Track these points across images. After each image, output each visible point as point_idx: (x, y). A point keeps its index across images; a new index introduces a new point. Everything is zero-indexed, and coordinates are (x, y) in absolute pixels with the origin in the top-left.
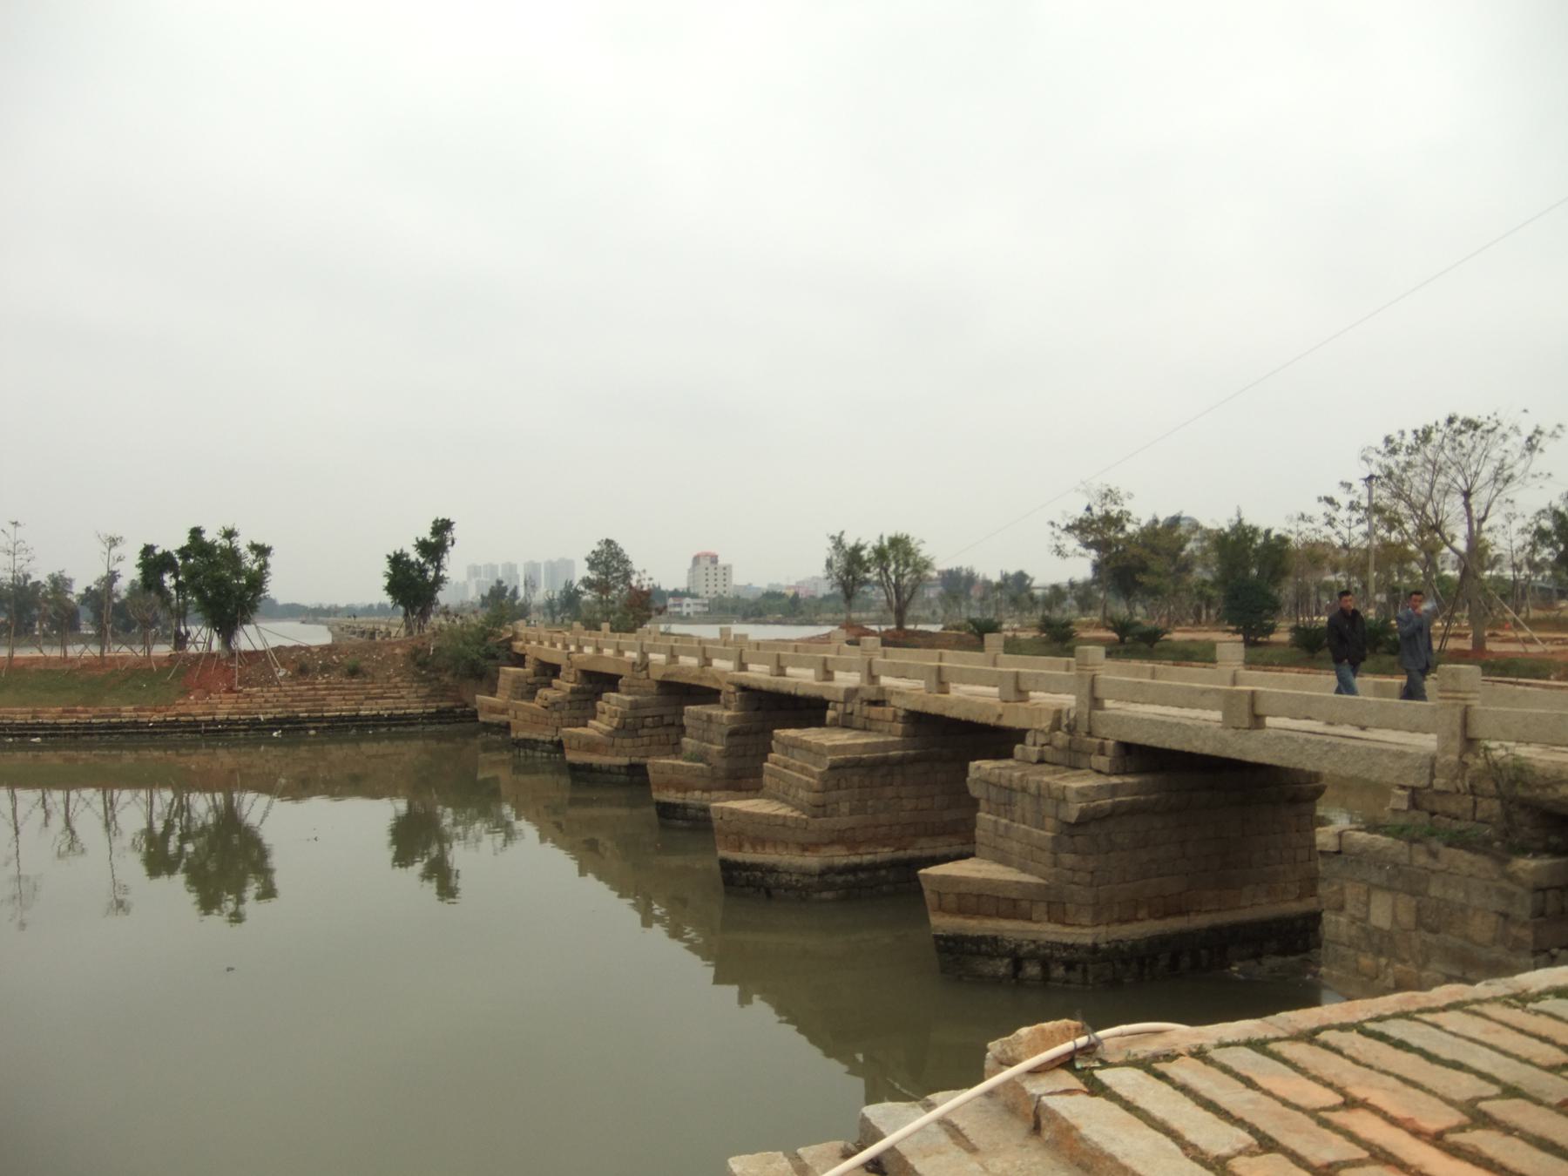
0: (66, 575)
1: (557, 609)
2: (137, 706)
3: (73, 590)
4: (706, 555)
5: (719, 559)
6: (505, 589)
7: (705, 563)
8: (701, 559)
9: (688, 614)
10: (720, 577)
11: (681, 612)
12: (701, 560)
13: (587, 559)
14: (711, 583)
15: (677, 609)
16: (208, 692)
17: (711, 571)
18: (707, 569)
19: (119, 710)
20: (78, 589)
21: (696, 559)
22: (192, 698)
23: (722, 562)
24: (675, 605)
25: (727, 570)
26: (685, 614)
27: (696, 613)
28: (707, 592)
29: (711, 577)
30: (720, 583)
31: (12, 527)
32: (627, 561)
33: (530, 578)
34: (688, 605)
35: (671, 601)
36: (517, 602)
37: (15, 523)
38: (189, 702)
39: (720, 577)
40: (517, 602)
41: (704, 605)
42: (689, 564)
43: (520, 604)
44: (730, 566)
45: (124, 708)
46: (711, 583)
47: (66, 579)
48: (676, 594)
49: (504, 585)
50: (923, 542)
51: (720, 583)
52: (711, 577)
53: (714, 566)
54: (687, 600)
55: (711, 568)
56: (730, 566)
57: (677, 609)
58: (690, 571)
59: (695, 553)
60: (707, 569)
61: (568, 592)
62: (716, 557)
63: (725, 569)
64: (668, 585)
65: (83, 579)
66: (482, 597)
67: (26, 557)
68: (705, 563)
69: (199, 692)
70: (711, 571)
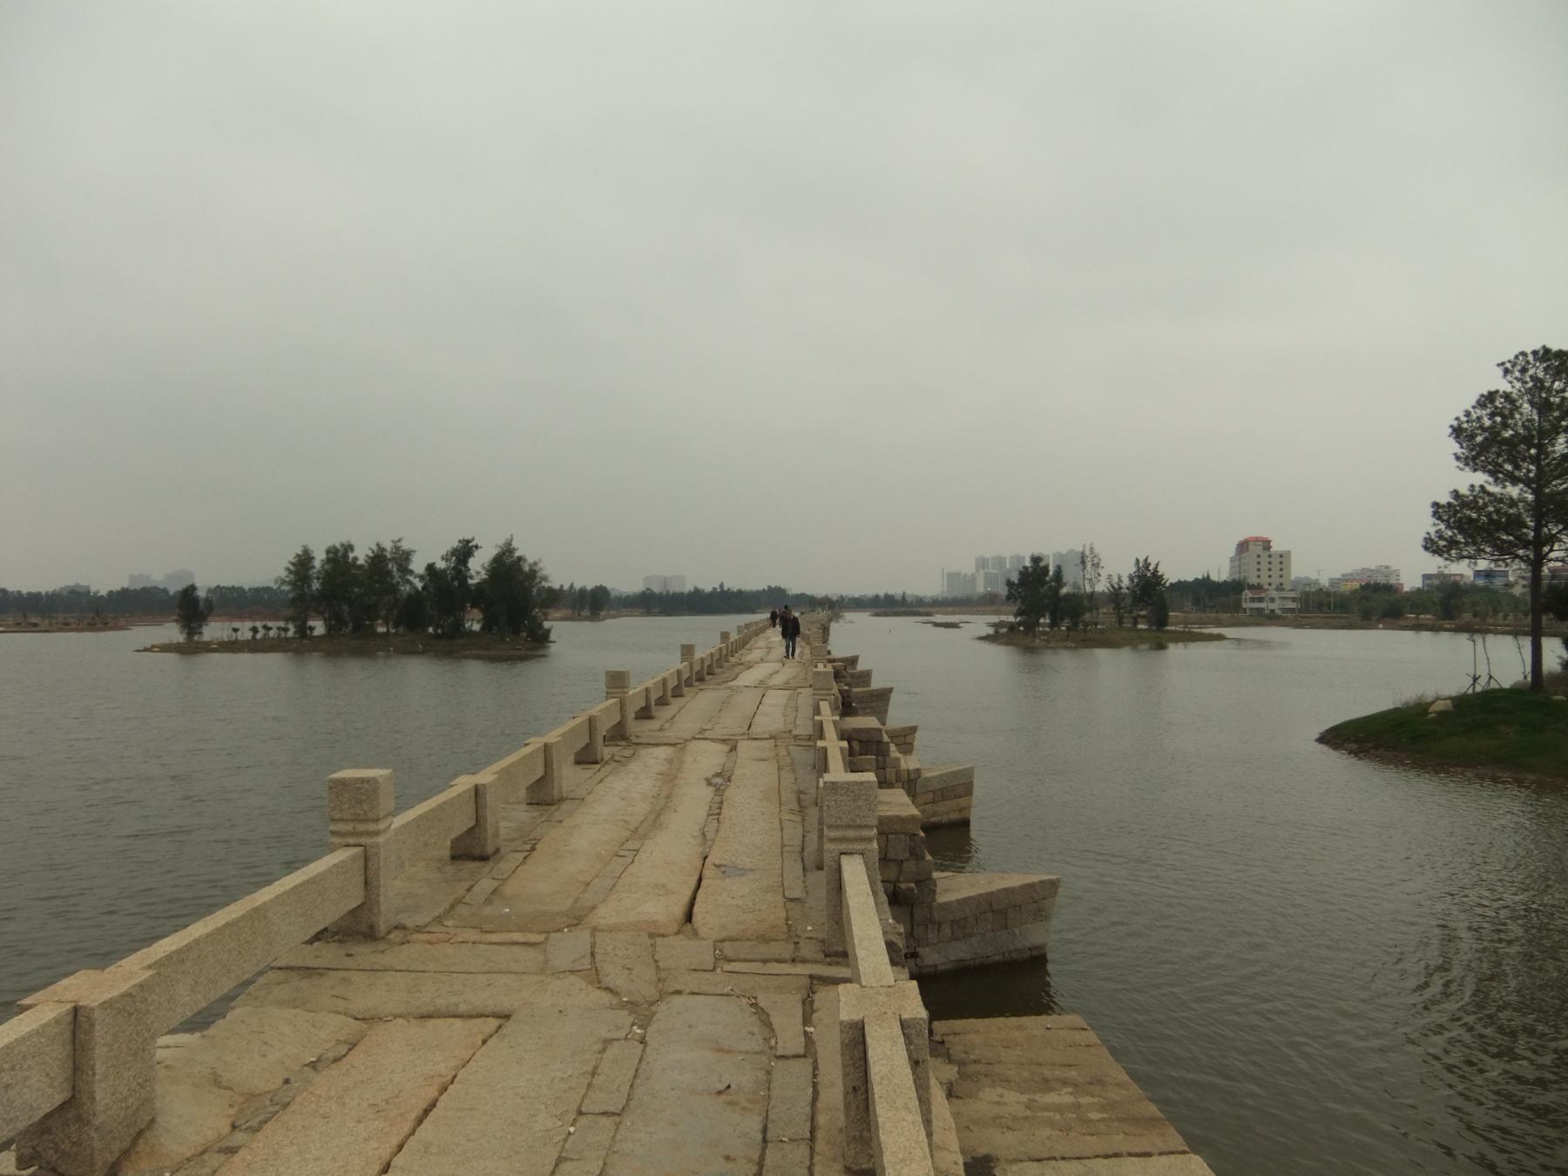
0: (405, 546)
1: (1129, 601)
3: (412, 567)
4: (1256, 540)
5: (1272, 544)
6: (1046, 569)
8: (1250, 543)
10: (1275, 566)
11: (1260, 610)
12: (1251, 547)
13: (1457, 432)
14: (1264, 573)
17: (1264, 559)
18: (1259, 556)
20: (418, 566)
21: (1243, 546)
23: (1276, 547)
24: (1253, 600)
25: (1284, 557)
29: (1264, 566)
30: (1275, 573)
33: (1092, 549)
39: (1275, 566)
40: (1064, 591)
41: (1294, 600)
42: (1232, 552)
46: (1264, 573)
47: (403, 551)
49: (1042, 564)
51: (1275, 573)
52: (1264, 566)
53: (1267, 553)
55: (1264, 555)
58: (1232, 560)
59: (1242, 539)
63: (1281, 556)
65: (429, 553)
66: (1009, 584)
68: (1255, 549)
70: (1264, 559)
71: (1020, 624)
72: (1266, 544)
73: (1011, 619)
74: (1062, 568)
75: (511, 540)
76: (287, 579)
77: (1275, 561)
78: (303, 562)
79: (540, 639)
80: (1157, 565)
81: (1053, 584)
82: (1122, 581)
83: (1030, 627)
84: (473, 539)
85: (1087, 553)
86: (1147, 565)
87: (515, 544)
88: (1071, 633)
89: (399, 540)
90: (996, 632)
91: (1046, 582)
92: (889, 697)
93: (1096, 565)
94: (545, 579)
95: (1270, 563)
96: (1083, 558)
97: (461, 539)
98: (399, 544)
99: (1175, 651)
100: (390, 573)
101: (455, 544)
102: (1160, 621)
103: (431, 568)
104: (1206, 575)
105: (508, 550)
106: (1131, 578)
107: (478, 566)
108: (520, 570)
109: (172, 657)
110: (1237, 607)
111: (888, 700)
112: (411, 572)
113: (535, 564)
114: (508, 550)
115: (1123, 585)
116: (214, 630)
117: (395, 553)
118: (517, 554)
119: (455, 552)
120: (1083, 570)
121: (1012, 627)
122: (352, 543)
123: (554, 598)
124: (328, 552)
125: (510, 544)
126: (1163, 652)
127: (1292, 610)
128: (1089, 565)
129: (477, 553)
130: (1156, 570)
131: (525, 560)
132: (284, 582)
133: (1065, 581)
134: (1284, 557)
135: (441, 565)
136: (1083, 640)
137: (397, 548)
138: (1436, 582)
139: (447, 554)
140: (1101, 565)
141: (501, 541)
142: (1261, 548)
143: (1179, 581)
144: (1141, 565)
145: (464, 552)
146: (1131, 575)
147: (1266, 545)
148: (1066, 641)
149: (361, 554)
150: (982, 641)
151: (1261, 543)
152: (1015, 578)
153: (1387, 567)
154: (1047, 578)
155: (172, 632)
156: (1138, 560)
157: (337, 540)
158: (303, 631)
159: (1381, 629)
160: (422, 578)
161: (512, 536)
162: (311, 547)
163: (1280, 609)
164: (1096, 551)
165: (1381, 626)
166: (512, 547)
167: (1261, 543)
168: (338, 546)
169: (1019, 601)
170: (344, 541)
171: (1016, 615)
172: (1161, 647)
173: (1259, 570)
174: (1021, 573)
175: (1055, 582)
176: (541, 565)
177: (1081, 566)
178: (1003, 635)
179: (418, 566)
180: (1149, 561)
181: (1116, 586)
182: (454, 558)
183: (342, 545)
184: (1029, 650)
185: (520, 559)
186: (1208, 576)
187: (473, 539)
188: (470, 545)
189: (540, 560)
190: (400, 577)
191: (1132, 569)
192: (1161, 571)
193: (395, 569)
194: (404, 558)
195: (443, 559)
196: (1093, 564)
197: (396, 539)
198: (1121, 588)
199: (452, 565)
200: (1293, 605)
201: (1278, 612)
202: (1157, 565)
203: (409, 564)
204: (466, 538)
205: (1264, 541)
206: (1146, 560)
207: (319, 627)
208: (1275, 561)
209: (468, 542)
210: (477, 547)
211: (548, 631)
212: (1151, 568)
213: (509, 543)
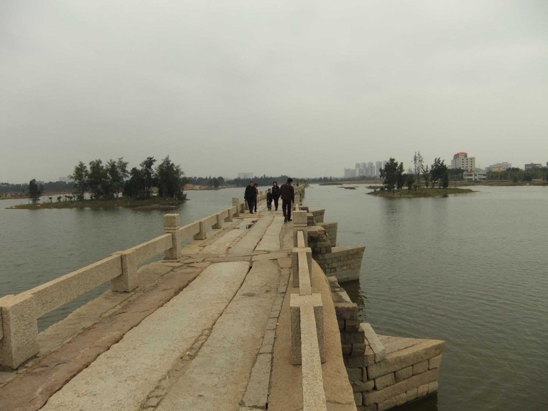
0: (124, 161)
1: (430, 177)
3: (127, 169)
4: (462, 153)
5: (467, 155)
6: (396, 164)
10: (469, 163)
12: (460, 156)
17: (465, 160)
18: (463, 159)
20: (129, 168)
21: (457, 156)
23: (469, 156)
24: (468, 175)
25: (472, 159)
27: (480, 179)
33: (419, 154)
36: (403, 173)
39: (469, 163)
40: (403, 173)
43: (405, 175)
47: (123, 163)
51: (469, 166)
55: (465, 159)
56: (474, 157)
58: (452, 161)
59: (456, 153)
60: (463, 159)
61: (437, 166)
63: (471, 159)
68: (461, 157)
70: (465, 160)
71: (385, 187)
73: (382, 185)
74: (403, 164)
75: (168, 157)
76: (73, 176)
77: (469, 161)
78: (80, 170)
79: (182, 199)
80: (443, 161)
81: (399, 170)
82: (428, 168)
83: (390, 189)
84: (153, 157)
85: (417, 156)
86: (439, 161)
87: (170, 159)
88: (410, 191)
89: (122, 158)
90: (375, 191)
91: (396, 169)
92: (362, 255)
93: (421, 161)
94: (182, 173)
96: (415, 158)
97: (148, 157)
98: (121, 160)
99: (452, 198)
100: (117, 172)
101: (146, 159)
102: (445, 185)
103: (134, 169)
105: (167, 161)
106: (432, 167)
107: (155, 167)
108: (173, 169)
109: (26, 211)
110: (462, 178)
111: (361, 258)
112: (127, 172)
113: (178, 167)
114: (167, 161)
115: (429, 170)
116: (43, 199)
117: (120, 164)
118: (171, 163)
119: (146, 163)
120: (415, 163)
121: (382, 189)
122: (101, 160)
123: (187, 181)
124: (90, 164)
125: (168, 159)
126: (447, 198)
127: (484, 179)
128: (418, 161)
129: (155, 163)
130: (442, 163)
131: (174, 166)
132: (72, 177)
133: (404, 169)
134: (472, 159)
135: (139, 168)
136: (415, 194)
137: (121, 162)
138: (530, 167)
139: (142, 163)
140: (423, 161)
141: (164, 158)
142: (463, 156)
144: (437, 161)
145: (149, 162)
146: (432, 165)
147: (466, 155)
148: (409, 194)
149: (105, 164)
150: (370, 195)
151: (464, 155)
152: (383, 168)
153: (507, 163)
154: (397, 168)
155: (27, 201)
156: (436, 159)
157: (94, 159)
158: (81, 198)
159: (528, 185)
160: (131, 174)
161: (168, 155)
162: (83, 162)
163: (479, 178)
164: (421, 155)
165: (528, 184)
166: (169, 160)
168: (95, 161)
169: (385, 177)
170: (98, 159)
171: (384, 184)
172: (446, 196)
174: (386, 166)
175: (400, 169)
176: (180, 167)
177: (414, 162)
178: (378, 192)
179: (129, 168)
180: (440, 159)
181: (425, 170)
182: (145, 165)
183: (96, 161)
184: (390, 198)
185: (173, 164)
187: (153, 157)
188: (152, 160)
189: (180, 165)
190: (123, 174)
191: (433, 163)
192: (445, 164)
193: (120, 171)
194: (123, 166)
195: (140, 165)
196: (420, 161)
197: (120, 158)
198: (427, 171)
199: (144, 168)
200: (485, 177)
201: (478, 180)
202: (443, 161)
203: (125, 168)
204: (150, 157)
205: (465, 154)
206: (439, 159)
207: (87, 196)
208: (469, 161)
209: (151, 159)
210: (155, 161)
211: (185, 195)
212: (441, 163)
213: (167, 158)
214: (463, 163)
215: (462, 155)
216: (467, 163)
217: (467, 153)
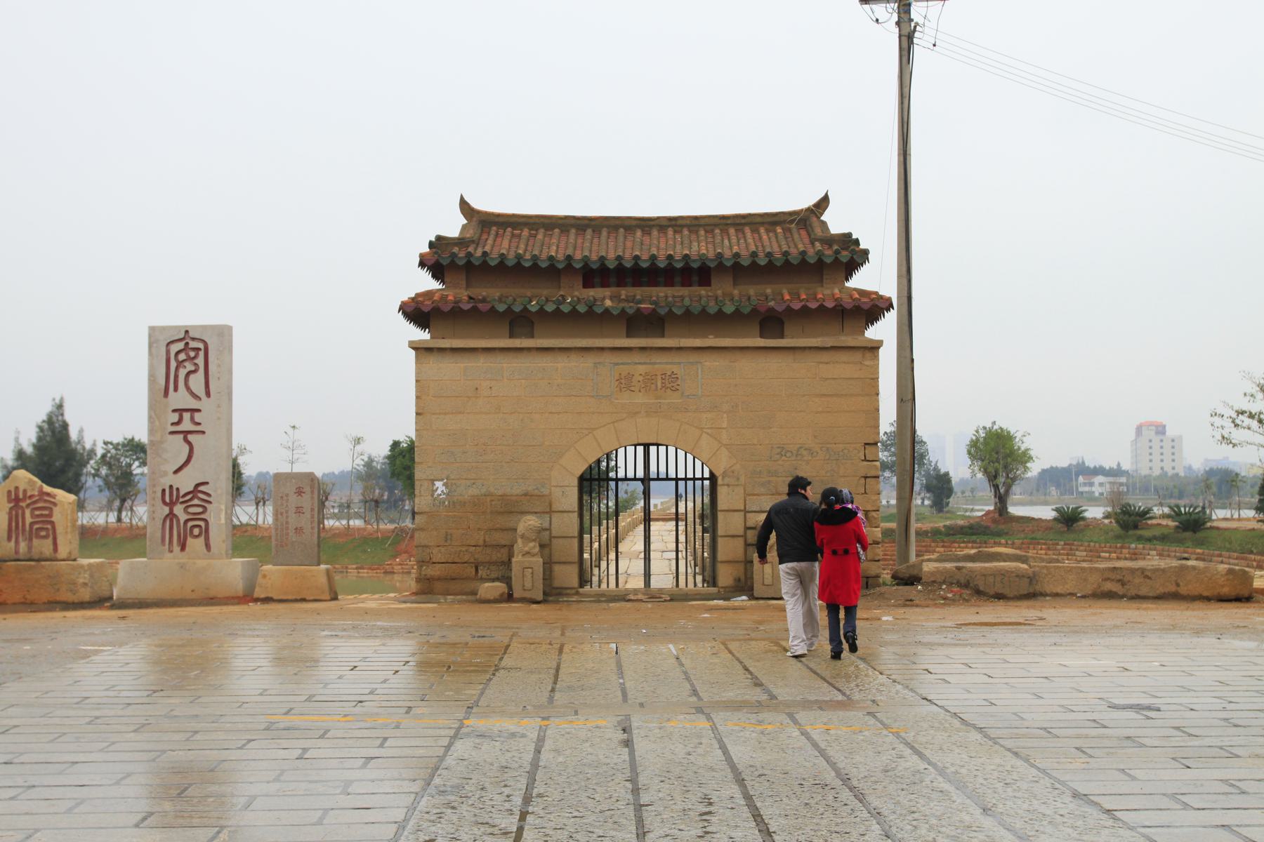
2: (359, 565)
4: (1149, 424)
5: (1167, 428)
7: (1149, 433)
8: (1143, 428)
9: (1101, 494)
14: (1156, 457)
15: (1087, 489)
16: (411, 556)
17: (1156, 444)
18: (1150, 441)
19: (347, 568)
21: (1139, 430)
22: (398, 560)
23: (1170, 432)
24: (1085, 484)
26: (1097, 494)
28: (1151, 468)
31: (292, 429)
32: (922, 441)
34: (1101, 484)
35: (1081, 479)
37: (294, 427)
38: (394, 563)
44: (1181, 437)
45: (350, 567)
46: (1156, 457)
48: (1098, 471)
50: (1029, 434)
53: (1160, 437)
54: (1100, 479)
55: (1156, 439)
56: (1181, 437)
57: (1087, 489)
60: (1150, 441)
62: (1164, 426)
63: (1173, 441)
64: (1090, 463)
67: (303, 451)
69: (405, 556)
70: (1156, 444)
72: (1160, 429)
80: (937, 462)
95: (1162, 447)
104: (1080, 461)
130: (936, 464)
142: (1153, 433)
143: (1052, 468)
147: (1161, 430)
167: (1154, 428)
173: (1151, 454)
186: (1083, 463)
202: (937, 462)
205: (1157, 427)
214: (1150, 451)
215: (1150, 428)
216: (1150, 451)
217: (1164, 423)
